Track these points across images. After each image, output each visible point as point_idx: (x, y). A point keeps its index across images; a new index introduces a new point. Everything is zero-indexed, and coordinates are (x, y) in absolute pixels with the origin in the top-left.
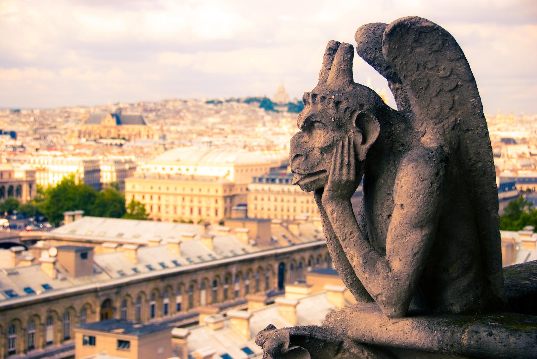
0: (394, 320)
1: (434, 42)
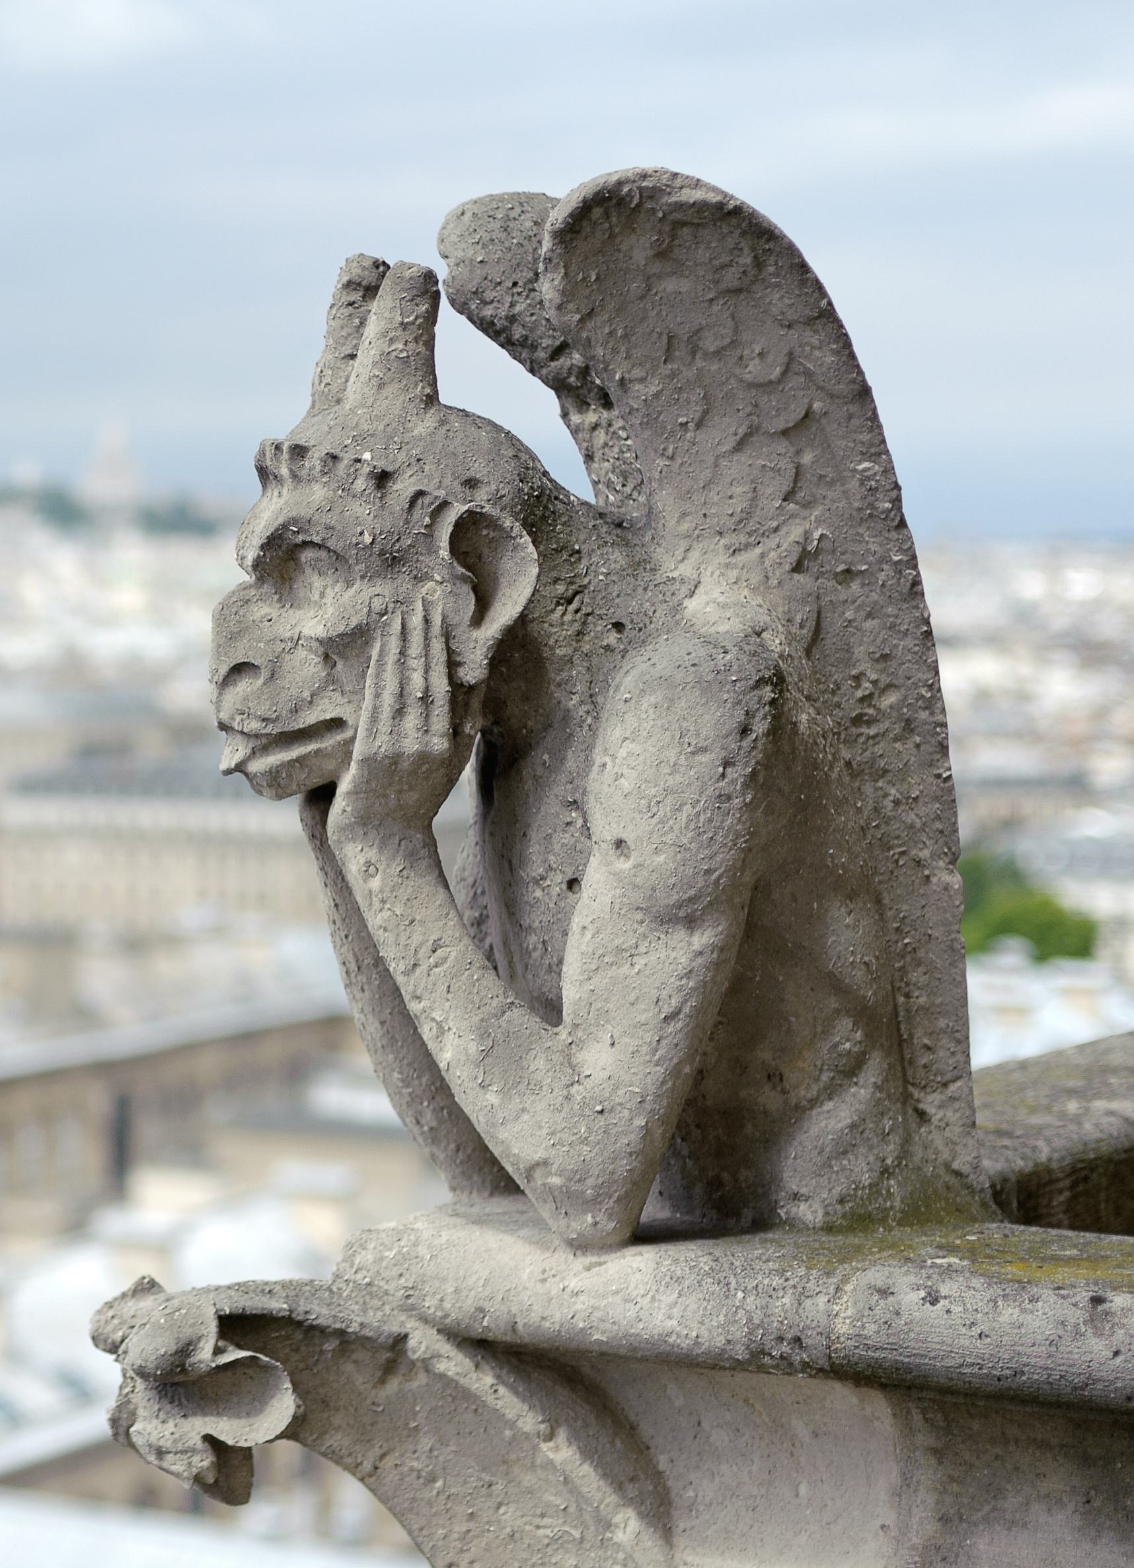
0: (591, 1259)
1: (725, 259)
